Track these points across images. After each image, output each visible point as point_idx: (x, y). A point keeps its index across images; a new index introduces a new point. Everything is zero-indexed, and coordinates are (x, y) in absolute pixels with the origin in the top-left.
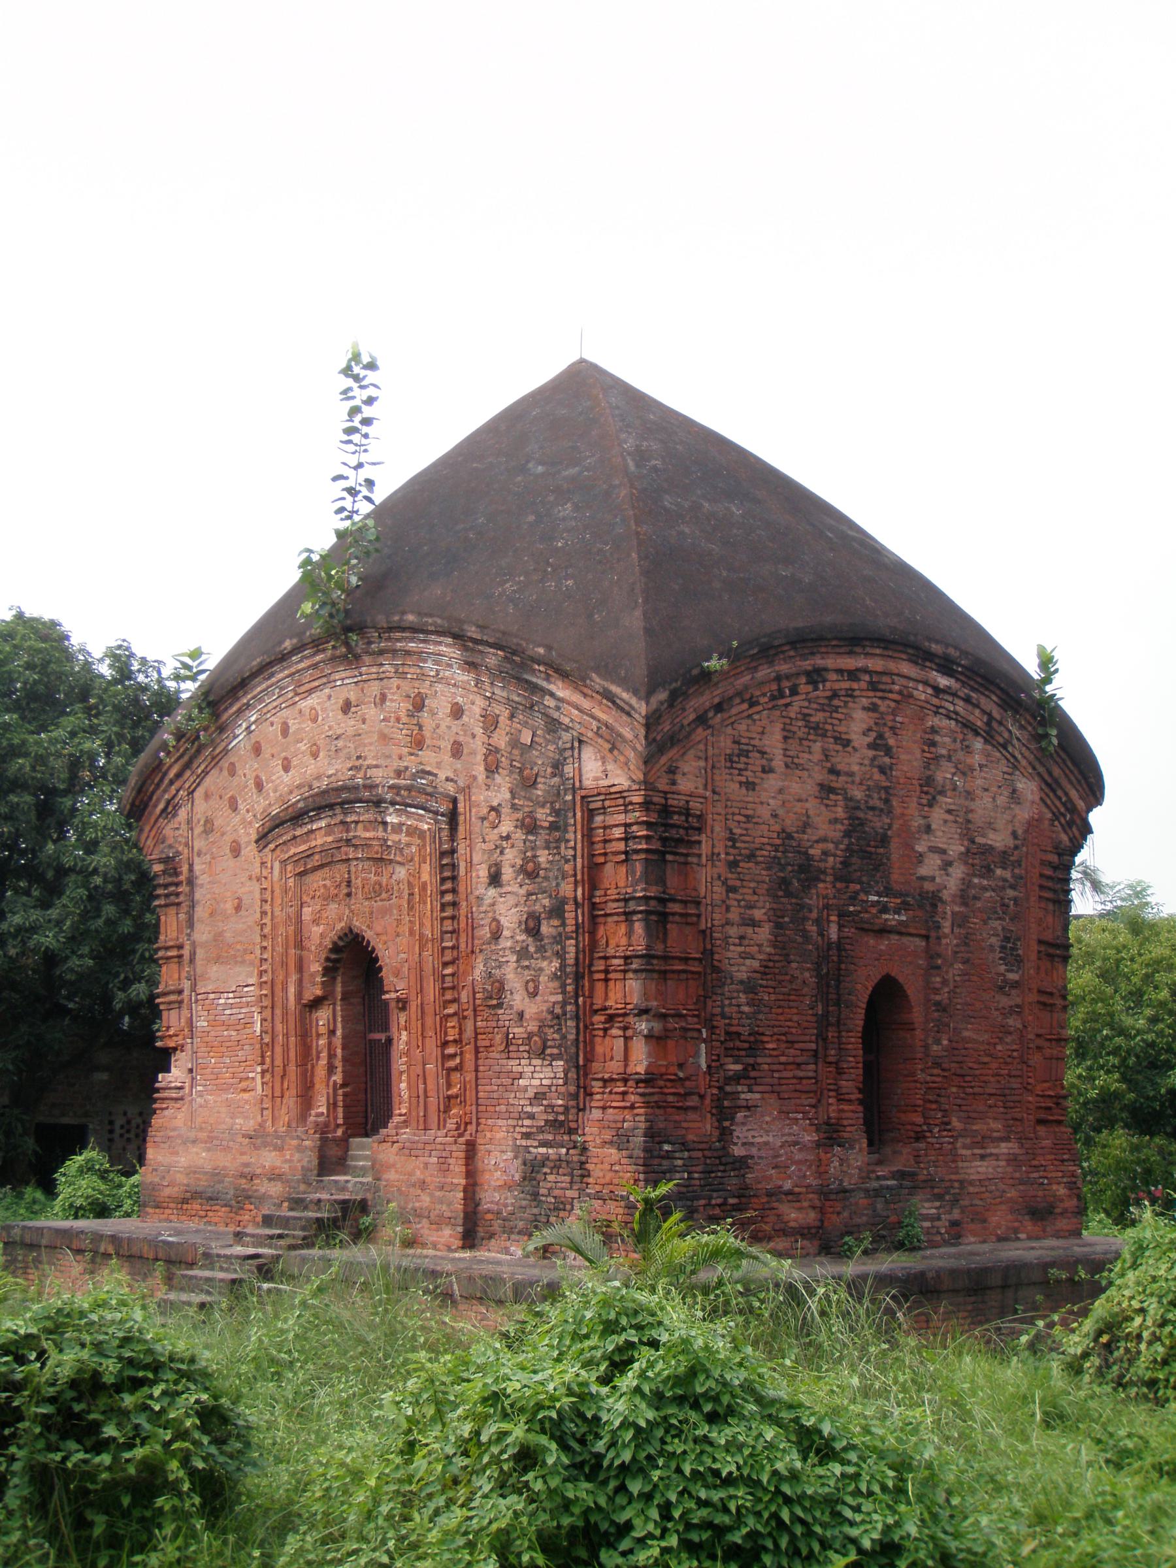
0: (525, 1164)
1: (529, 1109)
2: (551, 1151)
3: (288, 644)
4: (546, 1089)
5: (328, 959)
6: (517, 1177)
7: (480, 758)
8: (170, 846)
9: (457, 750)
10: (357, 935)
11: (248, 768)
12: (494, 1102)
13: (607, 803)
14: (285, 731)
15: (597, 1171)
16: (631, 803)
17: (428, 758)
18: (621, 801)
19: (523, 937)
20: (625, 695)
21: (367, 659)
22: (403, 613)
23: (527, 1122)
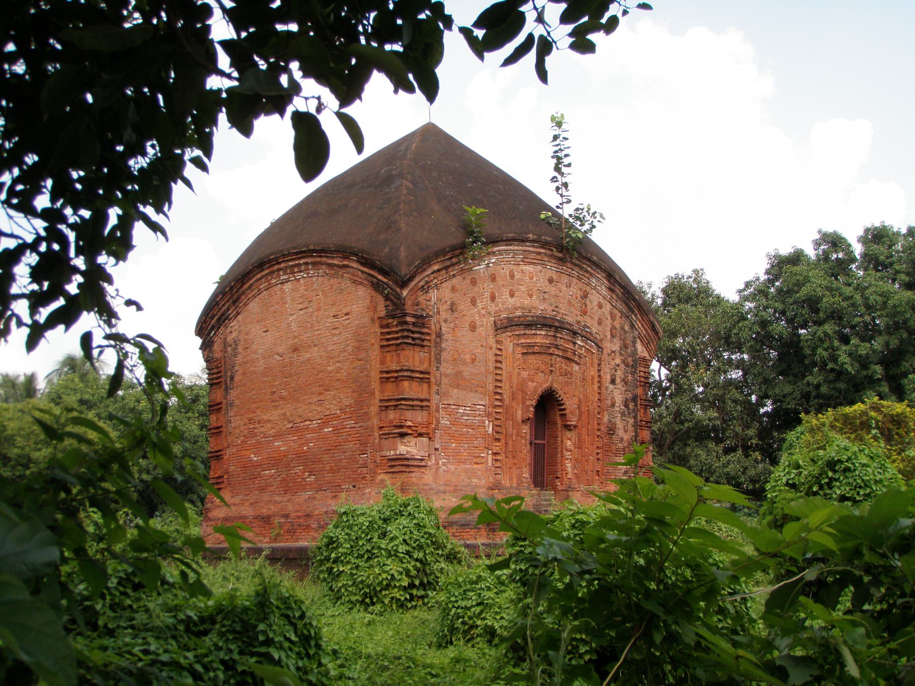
3: (530, 236)
7: (608, 329)
8: (423, 310)
9: (600, 323)
11: (487, 288)
14: (512, 276)
19: (623, 407)
21: (569, 265)
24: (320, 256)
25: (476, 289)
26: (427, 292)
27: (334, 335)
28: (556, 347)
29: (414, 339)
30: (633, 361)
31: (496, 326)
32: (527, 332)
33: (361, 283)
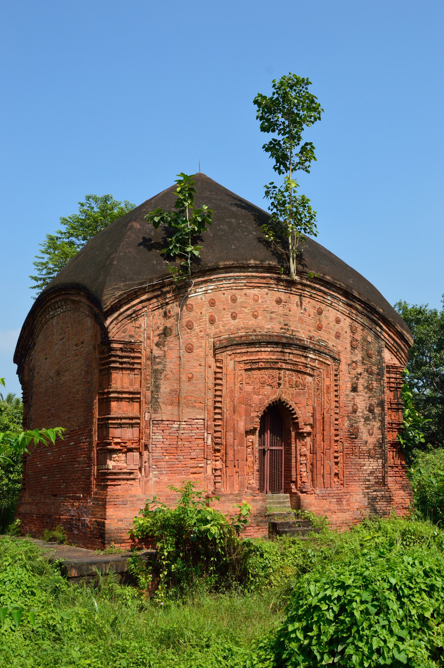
0: (368, 499)
1: (368, 478)
2: (378, 493)
3: (252, 262)
4: (375, 470)
5: (264, 412)
6: (366, 504)
7: (348, 341)
8: (131, 336)
9: (338, 336)
10: (284, 402)
12: (352, 476)
13: (391, 370)
14: (234, 300)
15: (397, 499)
16: (399, 371)
17: (323, 335)
18: (396, 370)
19: (367, 413)
20: (408, 336)
22: (324, 274)
23: (367, 483)
24: (67, 294)
25: (192, 314)
26: (135, 320)
27: (76, 361)
28: (285, 361)
29: (121, 363)
30: (378, 369)
31: (214, 346)
32: (250, 350)
33: (88, 316)
